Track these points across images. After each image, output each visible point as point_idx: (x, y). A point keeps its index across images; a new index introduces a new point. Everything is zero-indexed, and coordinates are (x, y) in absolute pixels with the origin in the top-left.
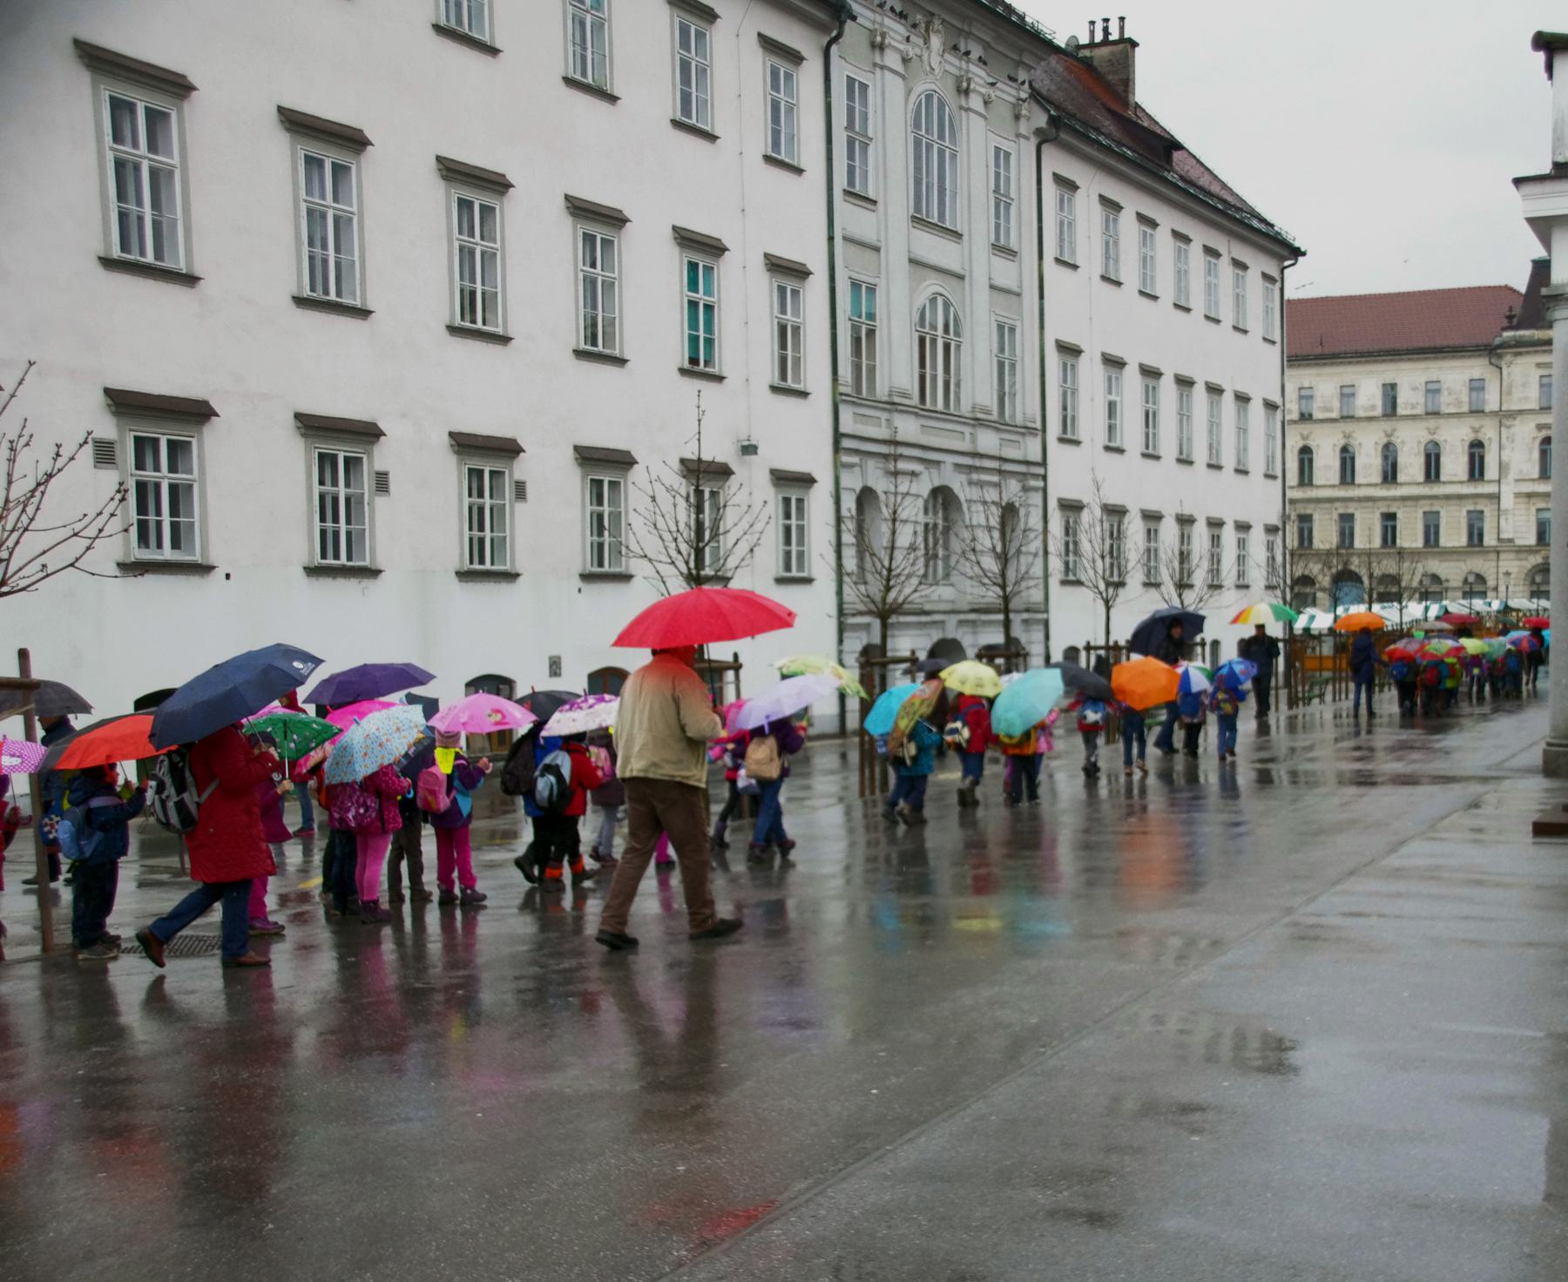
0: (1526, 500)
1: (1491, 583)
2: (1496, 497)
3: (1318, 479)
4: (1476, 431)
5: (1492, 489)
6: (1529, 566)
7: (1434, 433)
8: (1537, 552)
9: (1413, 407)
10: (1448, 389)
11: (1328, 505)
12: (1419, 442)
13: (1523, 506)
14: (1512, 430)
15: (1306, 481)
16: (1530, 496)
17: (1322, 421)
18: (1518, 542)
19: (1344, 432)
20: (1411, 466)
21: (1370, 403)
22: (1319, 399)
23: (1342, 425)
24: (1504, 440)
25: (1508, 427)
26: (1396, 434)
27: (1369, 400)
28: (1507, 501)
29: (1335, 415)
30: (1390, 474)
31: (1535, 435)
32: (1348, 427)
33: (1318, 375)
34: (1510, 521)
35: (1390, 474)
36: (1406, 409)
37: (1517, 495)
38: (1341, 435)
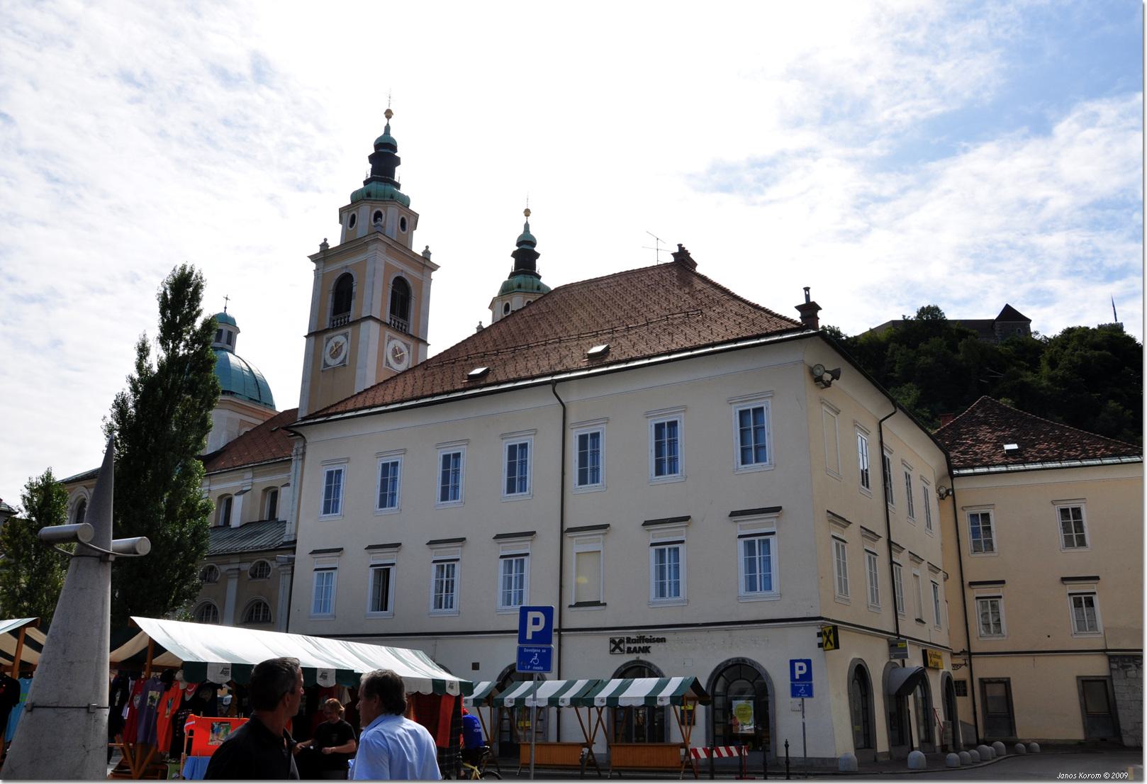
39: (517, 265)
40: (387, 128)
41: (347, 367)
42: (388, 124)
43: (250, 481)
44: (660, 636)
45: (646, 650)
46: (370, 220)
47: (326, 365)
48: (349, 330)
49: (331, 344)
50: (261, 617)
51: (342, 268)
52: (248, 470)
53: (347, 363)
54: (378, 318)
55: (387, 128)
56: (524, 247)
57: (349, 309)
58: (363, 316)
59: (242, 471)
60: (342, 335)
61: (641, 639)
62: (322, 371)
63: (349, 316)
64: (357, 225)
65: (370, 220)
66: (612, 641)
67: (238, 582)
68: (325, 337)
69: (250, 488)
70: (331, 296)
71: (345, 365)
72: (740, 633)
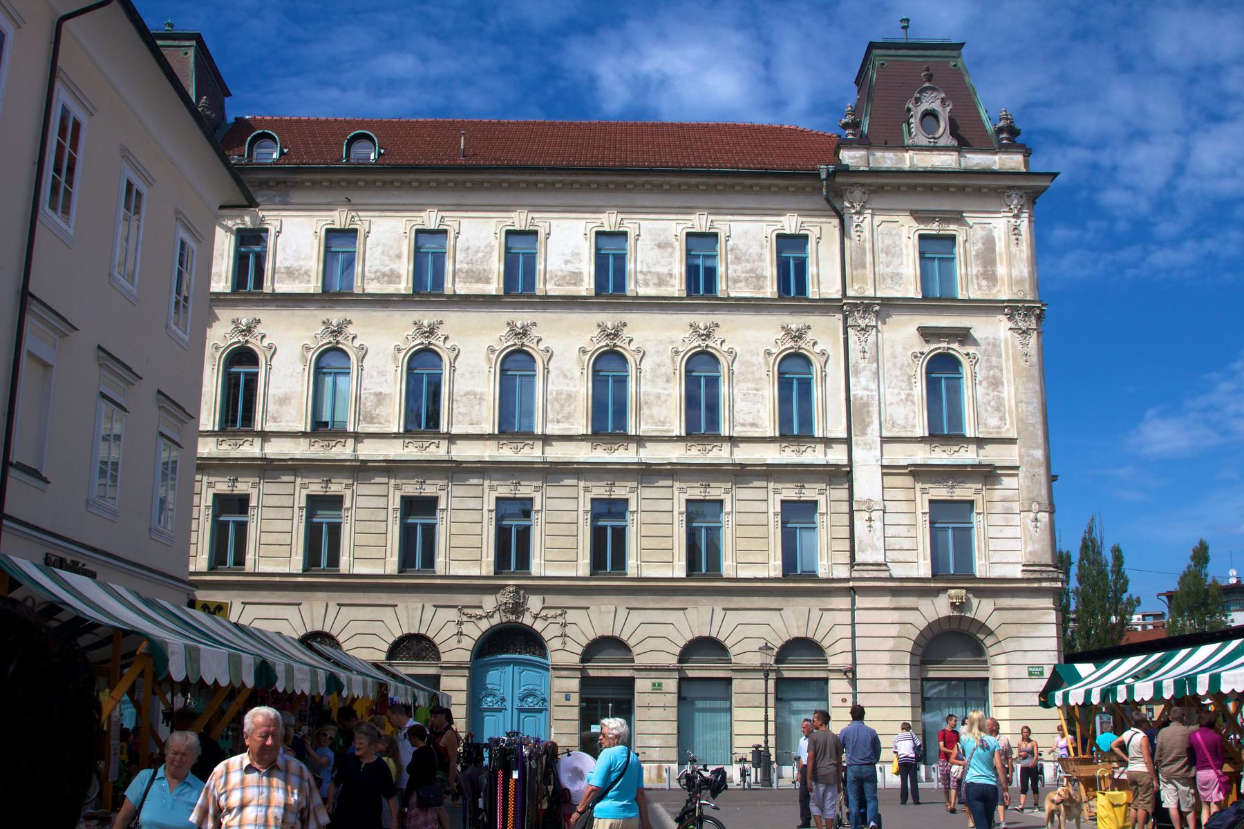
0: (908, 481)
1: (838, 658)
2: (841, 475)
3: (456, 418)
4: (799, 336)
5: (837, 455)
6: (923, 624)
7: (708, 336)
8: (935, 592)
9: (661, 282)
10: (732, 250)
12: (677, 352)
13: (901, 494)
14: (872, 337)
16: (920, 473)
18: (898, 571)
19: (511, 325)
21: (571, 268)
24: (854, 355)
25: (865, 330)
26: (626, 333)
27: (567, 262)
28: (867, 482)
31: (917, 350)
34: (877, 525)
36: (647, 284)
37: (888, 470)
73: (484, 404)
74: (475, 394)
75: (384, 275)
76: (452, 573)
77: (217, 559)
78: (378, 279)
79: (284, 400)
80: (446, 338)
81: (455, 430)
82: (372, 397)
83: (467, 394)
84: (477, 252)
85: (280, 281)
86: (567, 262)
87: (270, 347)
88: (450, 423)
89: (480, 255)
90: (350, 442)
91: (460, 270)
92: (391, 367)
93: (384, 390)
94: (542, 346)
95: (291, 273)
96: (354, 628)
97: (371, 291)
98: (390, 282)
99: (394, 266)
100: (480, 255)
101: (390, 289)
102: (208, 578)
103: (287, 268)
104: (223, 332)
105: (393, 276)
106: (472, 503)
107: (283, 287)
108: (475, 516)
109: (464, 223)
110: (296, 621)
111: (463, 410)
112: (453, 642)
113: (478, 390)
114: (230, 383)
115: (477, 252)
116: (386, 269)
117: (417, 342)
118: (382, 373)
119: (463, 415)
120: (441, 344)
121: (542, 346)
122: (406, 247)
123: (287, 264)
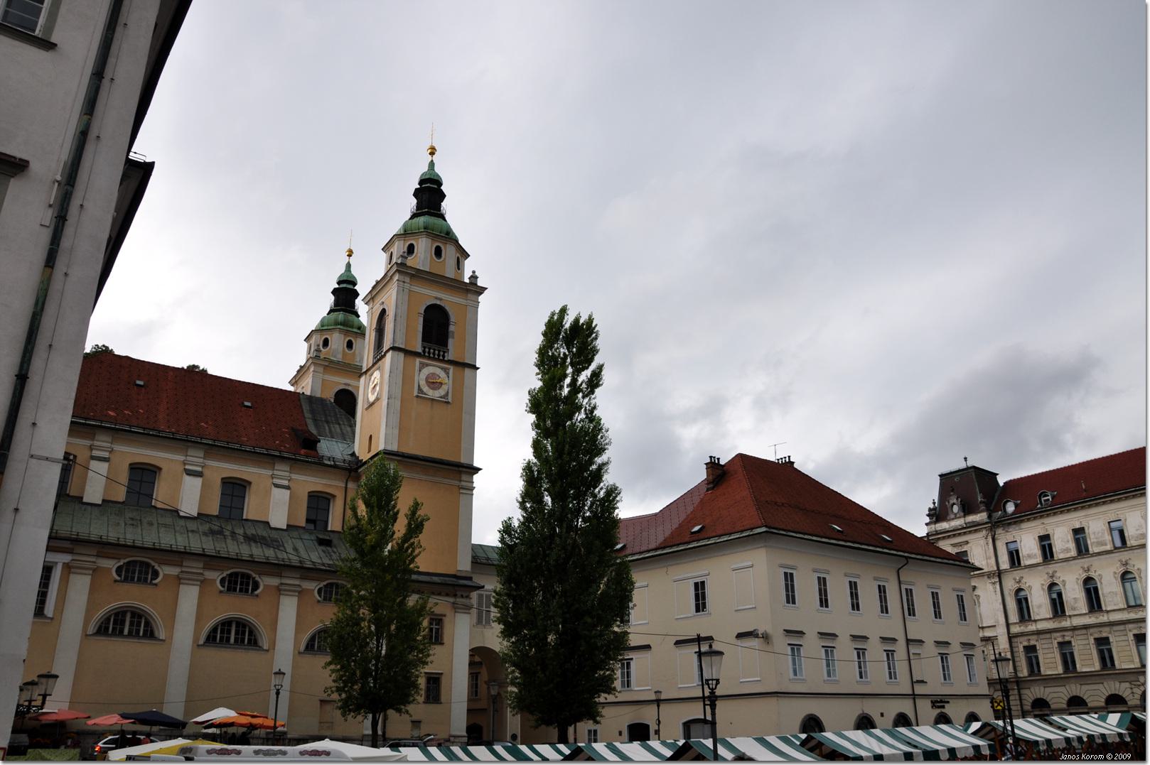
3: (1107, 603)
11: (1121, 627)
15: (1027, 617)
17: (1099, 554)
19: (1121, 561)
20: (1074, 595)
21: (1139, 532)
22: (1092, 536)
23: (1117, 554)
29: (1109, 547)
30: (1058, 606)
32: (1124, 556)
33: (1086, 516)
35: (1058, 606)
38: (1118, 564)
39: (337, 303)
40: (432, 164)
41: (449, 406)
42: (432, 161)
43: (201, 460)
44: (946, 700)
45: (943, 707)
46: (431, 255)
47: (420, 390)
48: (451, 368)
49: (426, 371)
50: (316, 646)
51: (436, 298)
52: (201, 446)
53: (450, 400)
54: (403, 346)
55: (432, 164)
56: (344, 285)
57: (446, 345)
58: (467, 361)
59: (190, 444)
60: (442, 368)
61: (941, 702)
62: (417, 396)
63: (444, 352)
64: (445, 259)
65: (431, 255)
66: (932, 702)
67: (92, 579)
68: (418, 360)
69: (199, 469)
70: (421, 320)
71: (448, 403)
72: (972, 701)
73: (1118, 596)
74: (1113, 592)
75: (1065, 550)
76: (1123, 667)
77: (1032, 672)
78: (1062, 552)
79: (1040, 606)
80: (1095, 571)
81: (1108, 609)
82: (1073, 600)
83: (1110, 593)
84: (1098, 533)
85: (1026, 560)
86: (1137, 530)
87: (1029, 586)
88: (1105, 606)
89: (1100, 534)
90: (1068, 618)
91: (1094, 542)
92: (1076, 587)
93: (1076, 596)
94: (1136, 568)
95: (1029, 556)
96: (1089, 693)
97: (1061, 558)
98: (1068, 552)
99: (1067, 546)
100: (1100, 534)
101: (1068, 555)
102: (1029, 679)
103: (1028, 555)
104: (1010, 584)
105: (1068, 550)
106: (1123, 638)
107: (1028, 562)
108: (1126, 643)
109: (1090, 523)
110: (1066, 692)
111: (1110, 599)
112: (1131, 696)
113: (1114, 590)
114: (1019, 602)
115: (1098, 533)
116: (1064, 548)
117: (1084, 576)
118: (1074, 590)
119: (1110, 601)
120: (1093, 574)
121: (1136, 568)
122: (1070, 536)
123: (1027, 553)
